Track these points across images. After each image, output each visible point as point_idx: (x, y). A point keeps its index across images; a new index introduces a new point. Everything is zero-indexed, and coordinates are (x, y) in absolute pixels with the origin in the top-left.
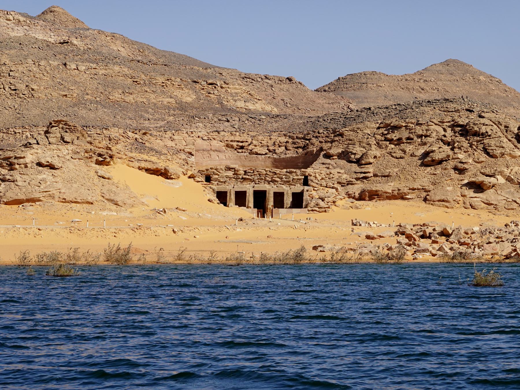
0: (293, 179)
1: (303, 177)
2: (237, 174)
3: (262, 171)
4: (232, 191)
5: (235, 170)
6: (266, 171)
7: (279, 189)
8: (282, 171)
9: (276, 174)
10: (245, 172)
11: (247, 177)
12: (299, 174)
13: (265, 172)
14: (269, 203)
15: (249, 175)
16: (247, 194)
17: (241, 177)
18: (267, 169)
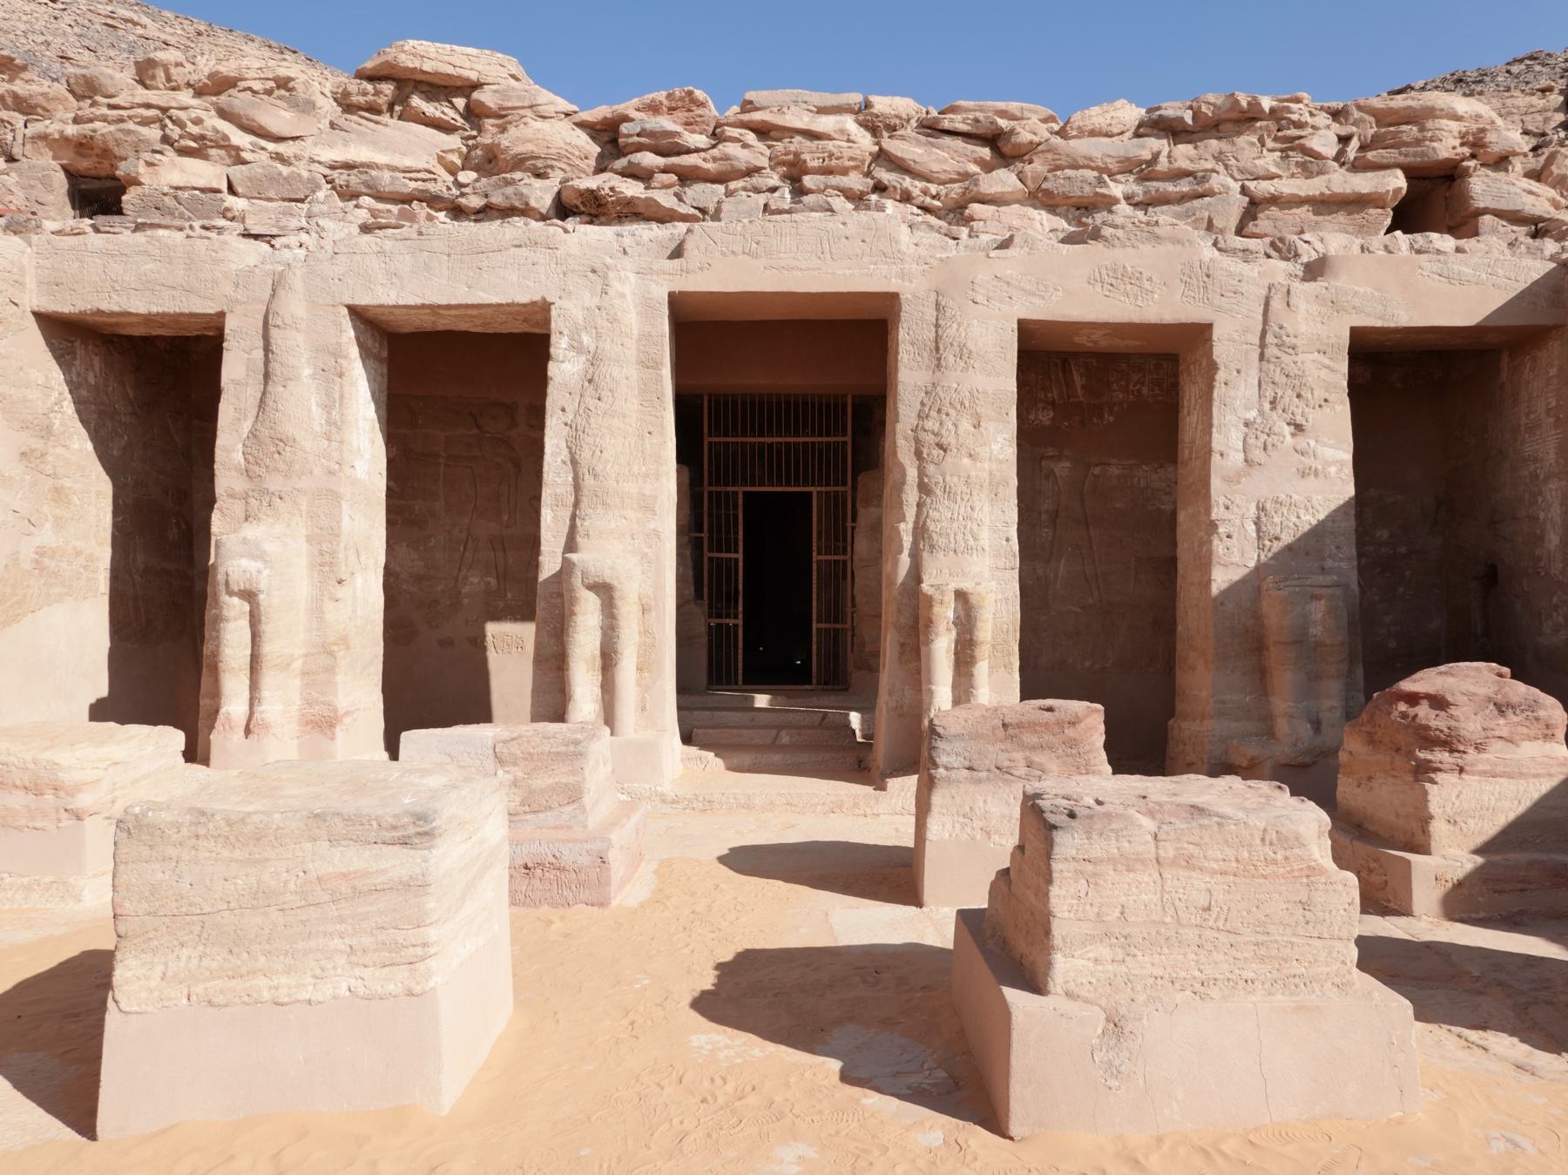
0: (1254, 206)
1: (1397, 182)
2: (491, 163)
3: (825, 123)
4: (294, 306)
5: (474, 114)
6: (873, 127)
7: (1118, 278)
8: (1096, 116)
9: (999, 146)
10: (608, 135)
11: (632, 189)
12: (1324, 142)
13: (865, 142)
14: (941, 516)
15: (644, 176)
16: (564, 369)
17: (541, 194)
18: (883, 104)
